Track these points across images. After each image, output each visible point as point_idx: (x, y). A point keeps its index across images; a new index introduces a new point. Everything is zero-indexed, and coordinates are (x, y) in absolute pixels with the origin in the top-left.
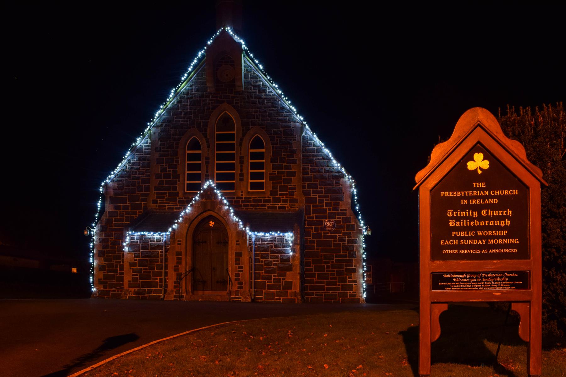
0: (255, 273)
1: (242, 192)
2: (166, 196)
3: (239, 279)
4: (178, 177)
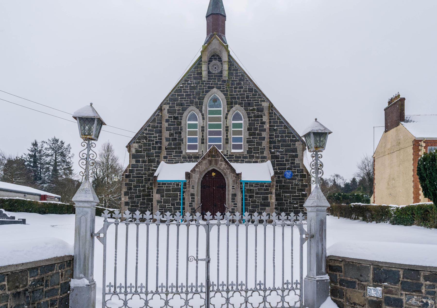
0: (245, 208)
2: (174, 154)
3: (192, 206)
4: (182, 140)
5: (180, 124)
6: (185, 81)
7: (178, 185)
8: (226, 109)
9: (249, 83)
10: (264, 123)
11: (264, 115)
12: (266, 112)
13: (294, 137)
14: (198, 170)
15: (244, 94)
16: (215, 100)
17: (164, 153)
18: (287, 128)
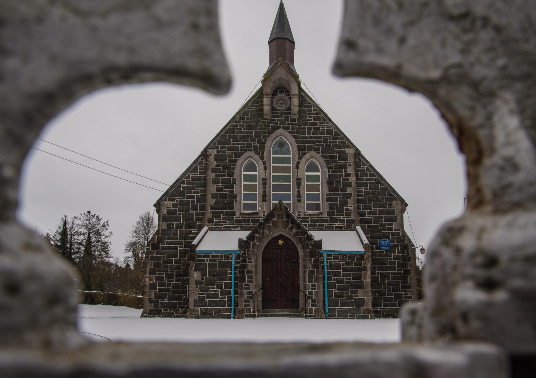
1: (299, 212)
4: (235, 197)
5: (232, 175)
6: (241, 118)
7: (227, 258)
8: (297, 156)
9: (327, 123)
10: (349, 175)
11: (349, 165)
12: (351, 160)
13: (389, 194)
14: (258, 235)
15: (321, 138)
16: (282, 144)
17: (209, 214)
18: (379, 182)
